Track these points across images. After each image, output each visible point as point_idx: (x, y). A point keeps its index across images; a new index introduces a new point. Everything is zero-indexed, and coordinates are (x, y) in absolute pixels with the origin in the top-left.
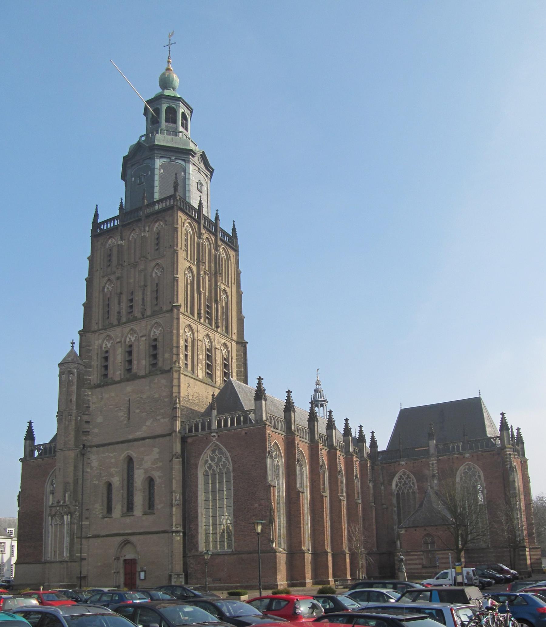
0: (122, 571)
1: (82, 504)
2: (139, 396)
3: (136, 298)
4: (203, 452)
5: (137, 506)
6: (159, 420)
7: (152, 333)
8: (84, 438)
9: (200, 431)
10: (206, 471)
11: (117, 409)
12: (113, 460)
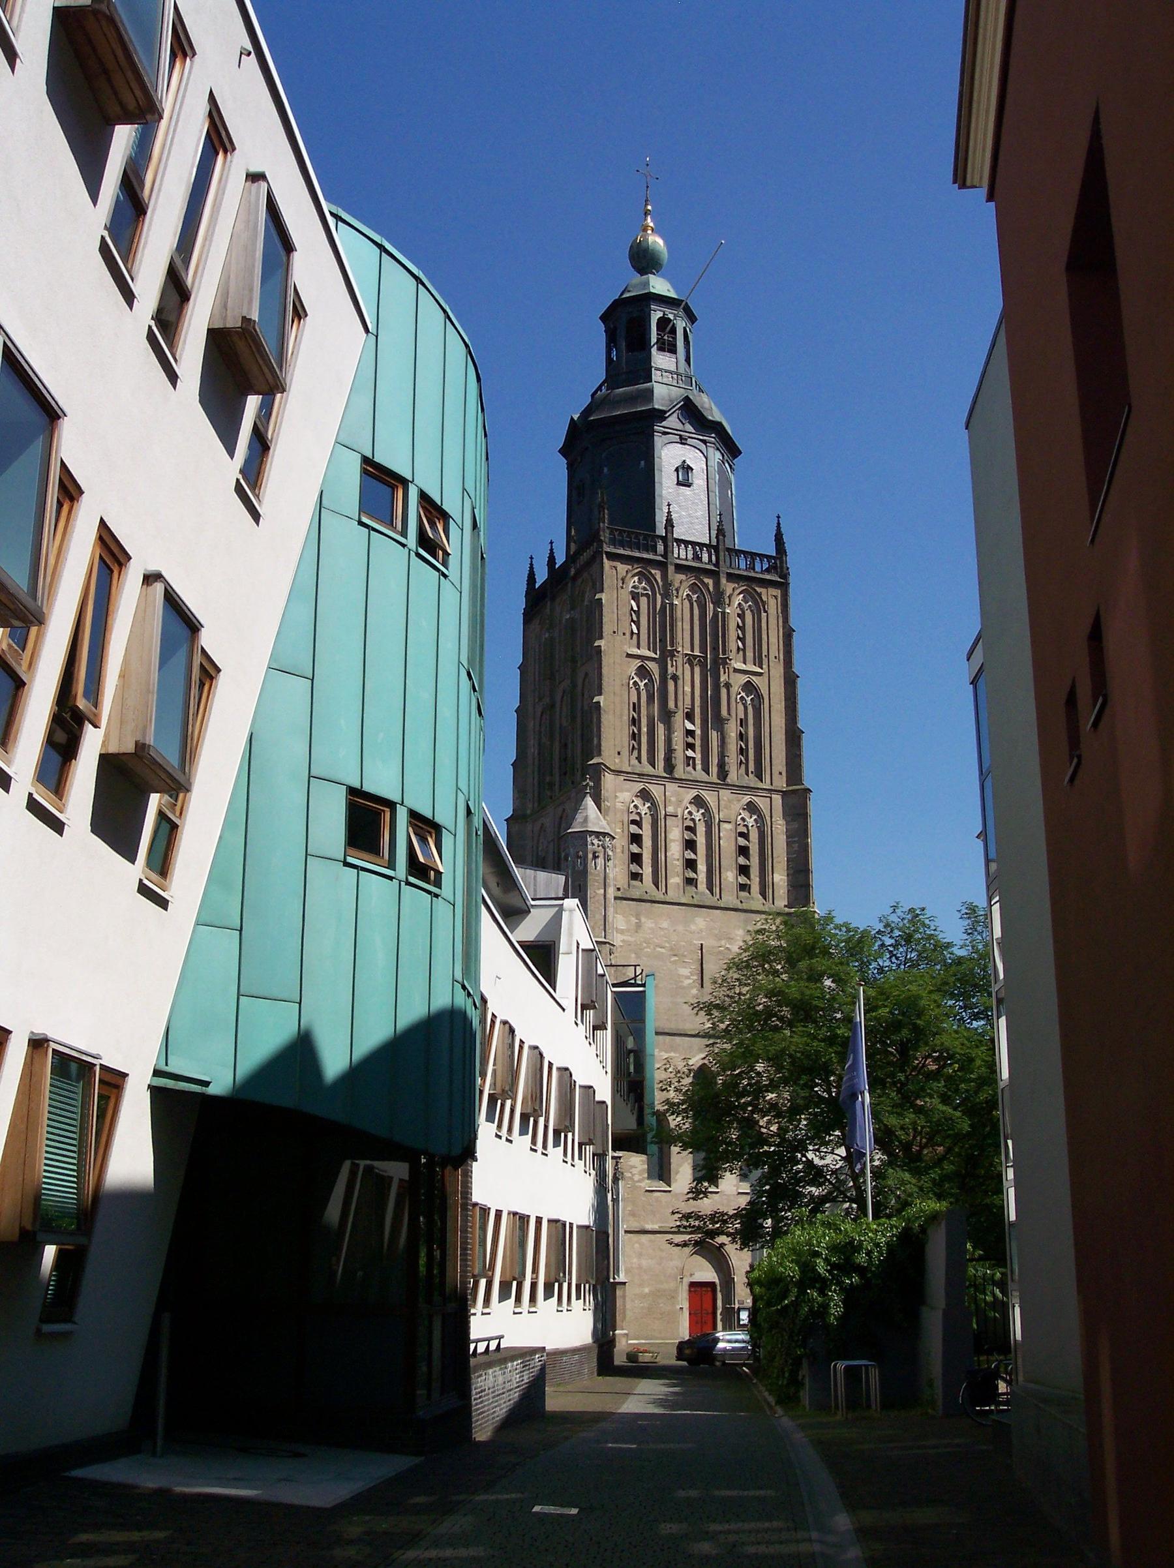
2: (723, 942)
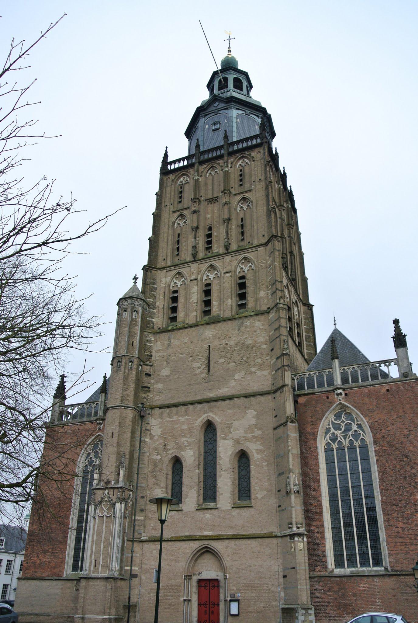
0: (195, 599)
1: (137, 488)
2: (224, 341)
3: (215, 234)
4: (324, 416)
5: (222, 494)
6: (255, 373)
7: (238, 270)
8: (144, 395)
9: (316, 387)
10: (328, 444)
11: (192, 358)
12: (185, 427)
